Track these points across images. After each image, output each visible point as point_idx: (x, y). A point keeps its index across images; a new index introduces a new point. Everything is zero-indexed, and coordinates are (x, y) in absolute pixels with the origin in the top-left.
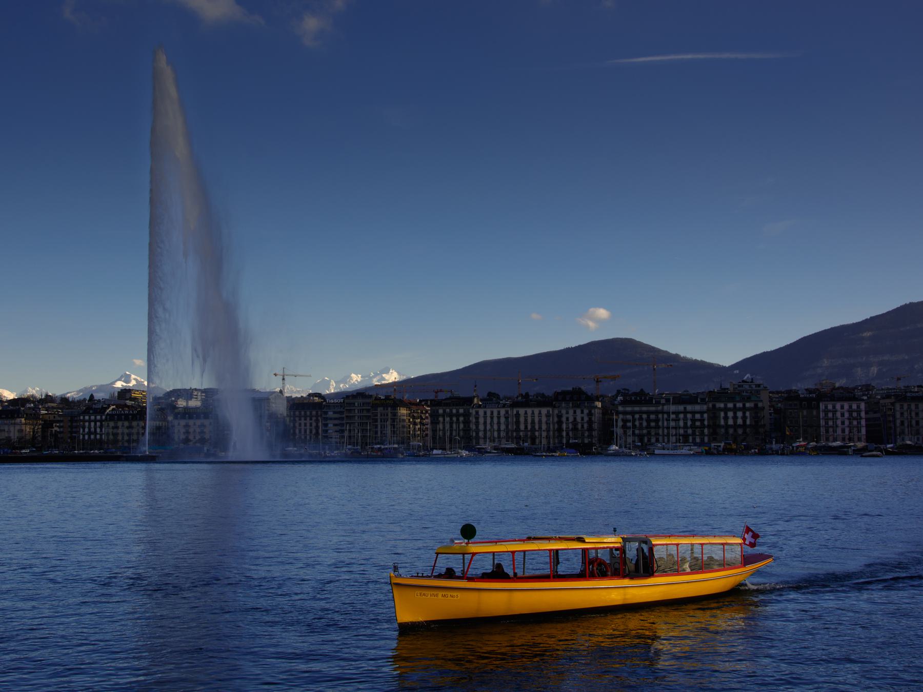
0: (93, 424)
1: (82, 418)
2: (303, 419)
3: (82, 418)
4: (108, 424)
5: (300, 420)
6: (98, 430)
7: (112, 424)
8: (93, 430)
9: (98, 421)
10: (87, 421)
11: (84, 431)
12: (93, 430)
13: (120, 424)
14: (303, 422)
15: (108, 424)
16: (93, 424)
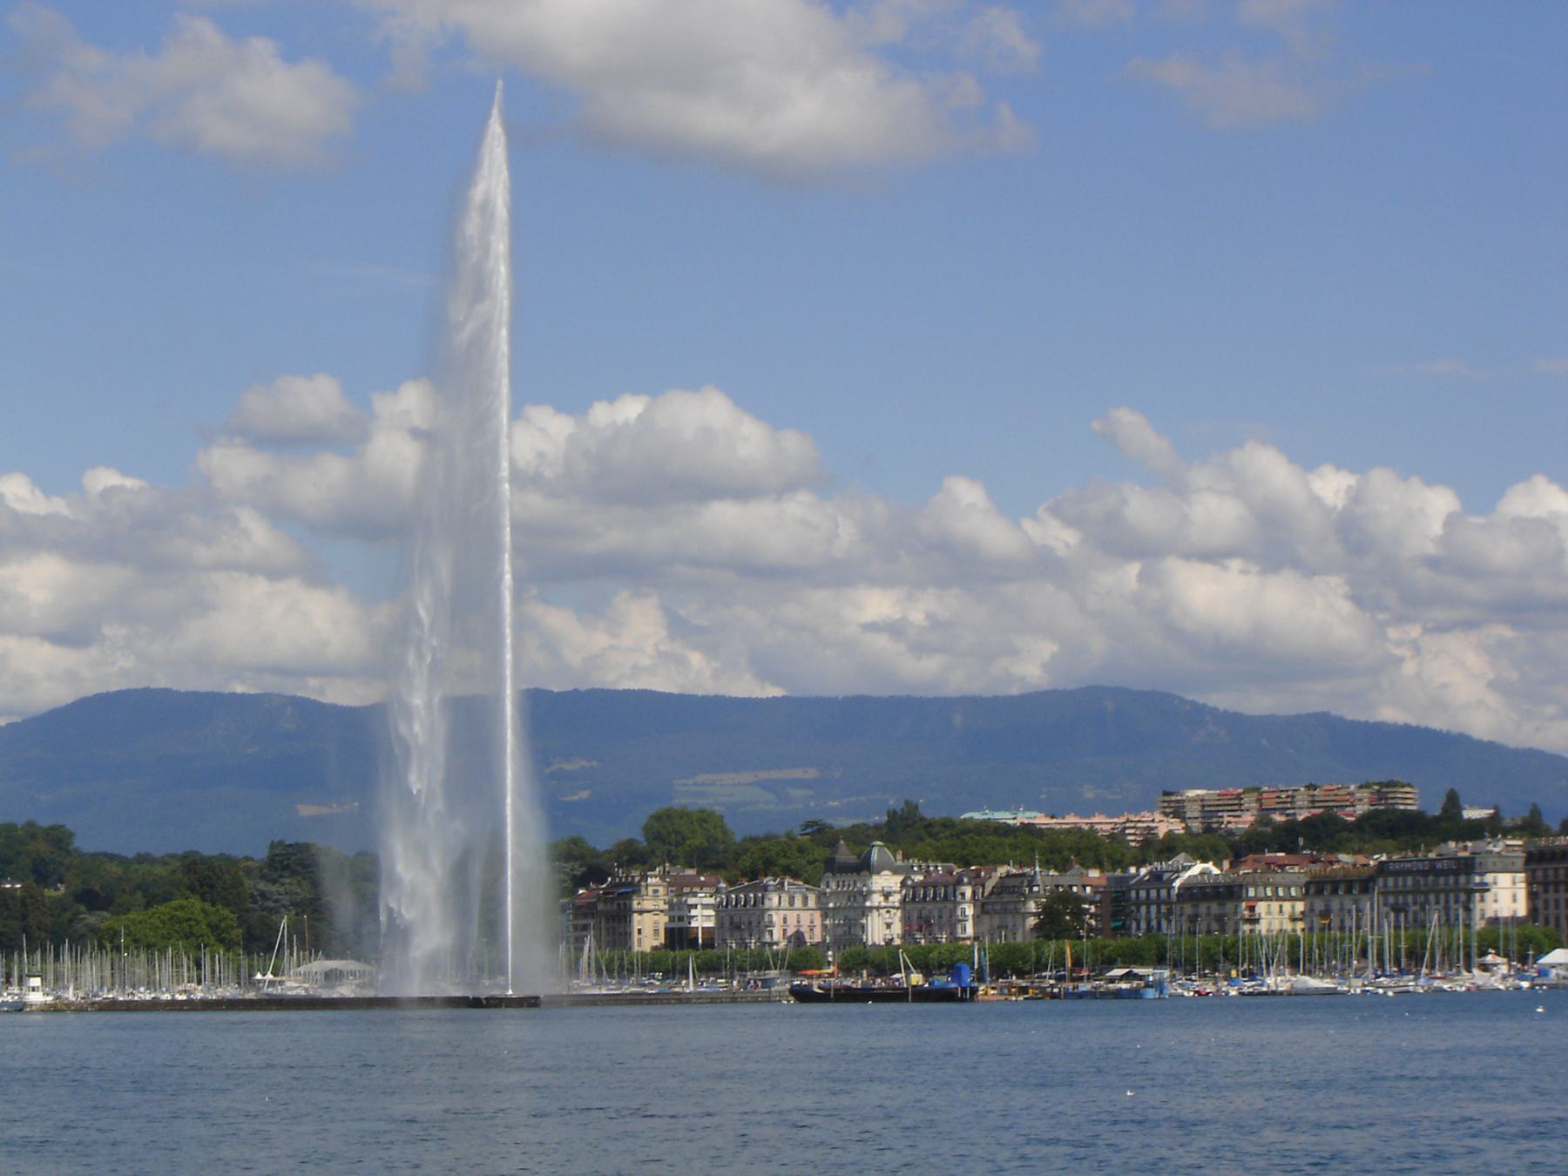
0: (1153, 909)
1: (1133, 894)
2: (1551, 888)
3: (1133, 894)
4: (1182, 908)
5: (1546, 891)
6: (1164, 923)
7: (1188, 909)
8: (1154, 923)
9: (1165, 903)
10: (1142, 903)
11: (1138, 928)
12: (1154, 923)
13: (1203, 908)
14: (1551, 896)
15: (1182, 908)
16: (1153, 909)
